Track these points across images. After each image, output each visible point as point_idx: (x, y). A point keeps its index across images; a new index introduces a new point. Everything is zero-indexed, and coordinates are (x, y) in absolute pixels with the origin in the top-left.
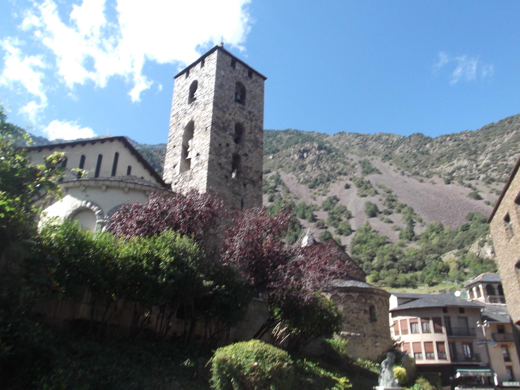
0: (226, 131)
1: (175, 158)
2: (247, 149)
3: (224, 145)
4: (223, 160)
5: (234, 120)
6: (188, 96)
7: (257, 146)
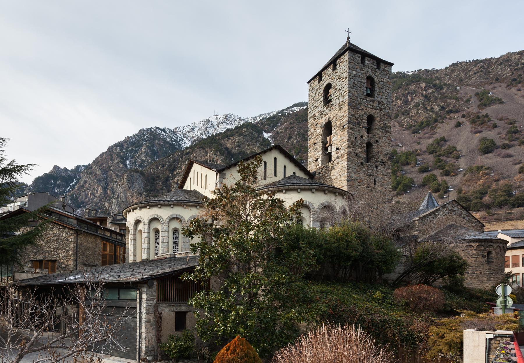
1: (316, 153)
3: (359, 137)
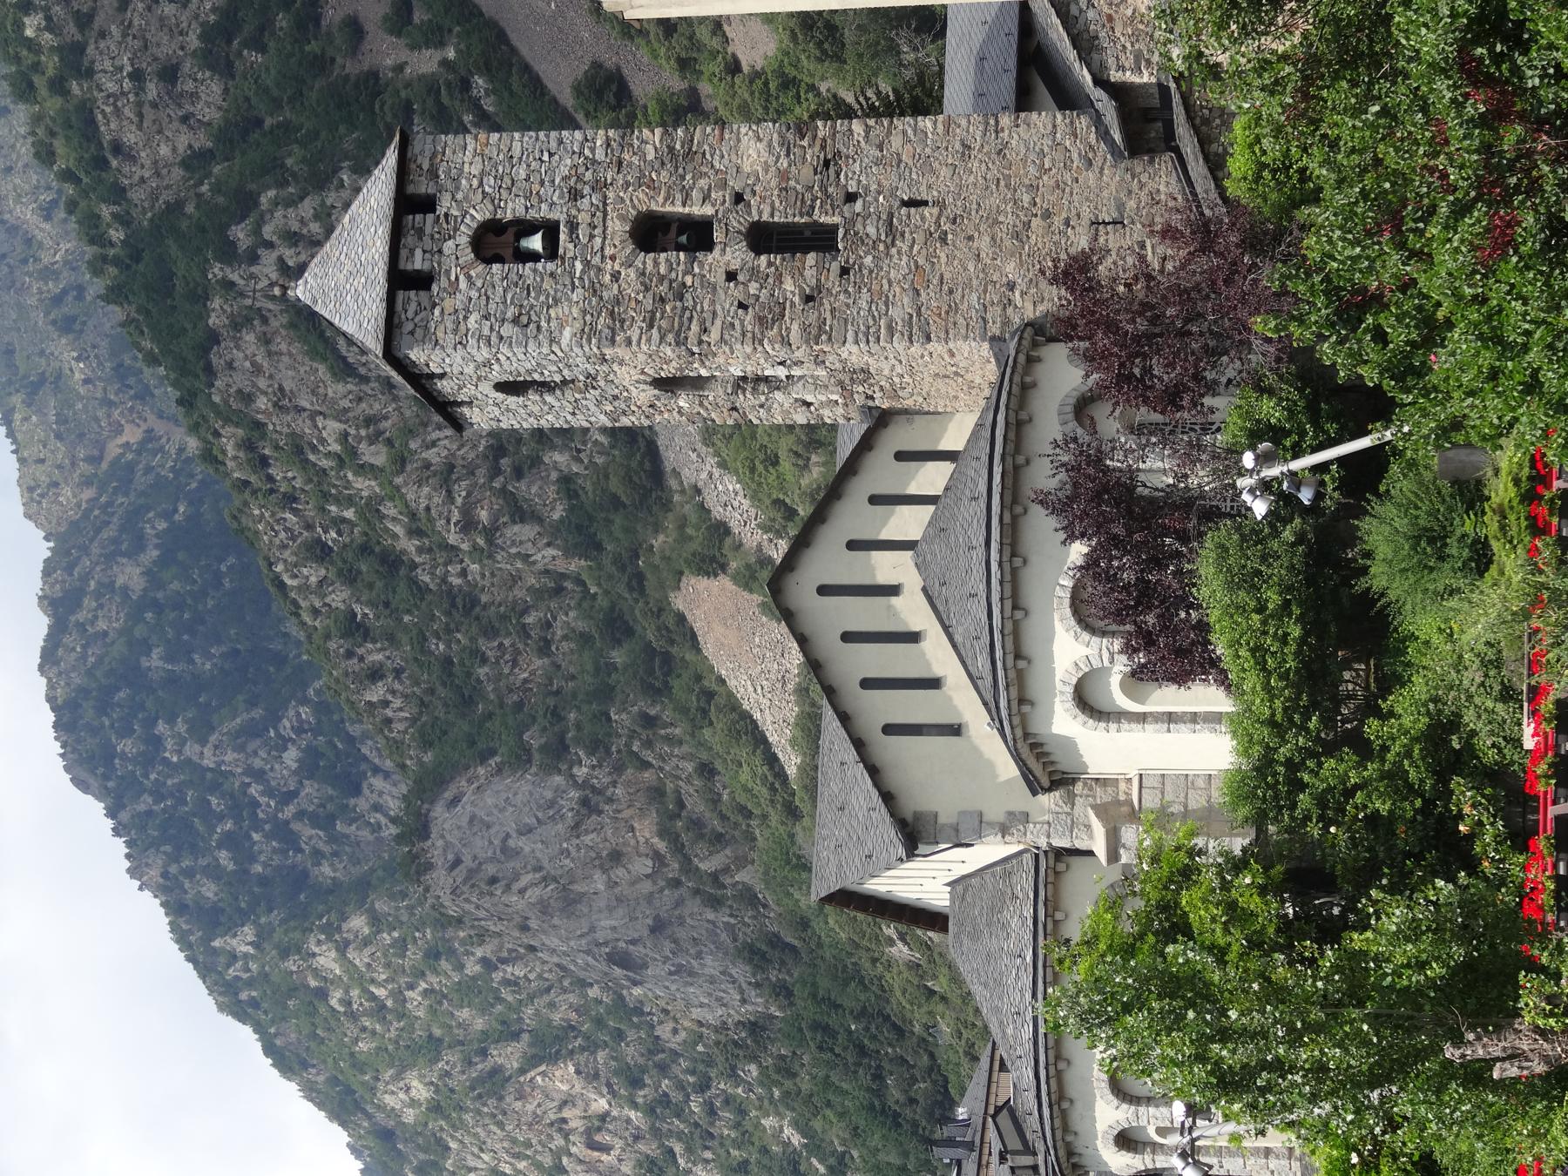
0: (684, 284)
3: (735, 291)
6: (549, 398)
7: (689, 154)
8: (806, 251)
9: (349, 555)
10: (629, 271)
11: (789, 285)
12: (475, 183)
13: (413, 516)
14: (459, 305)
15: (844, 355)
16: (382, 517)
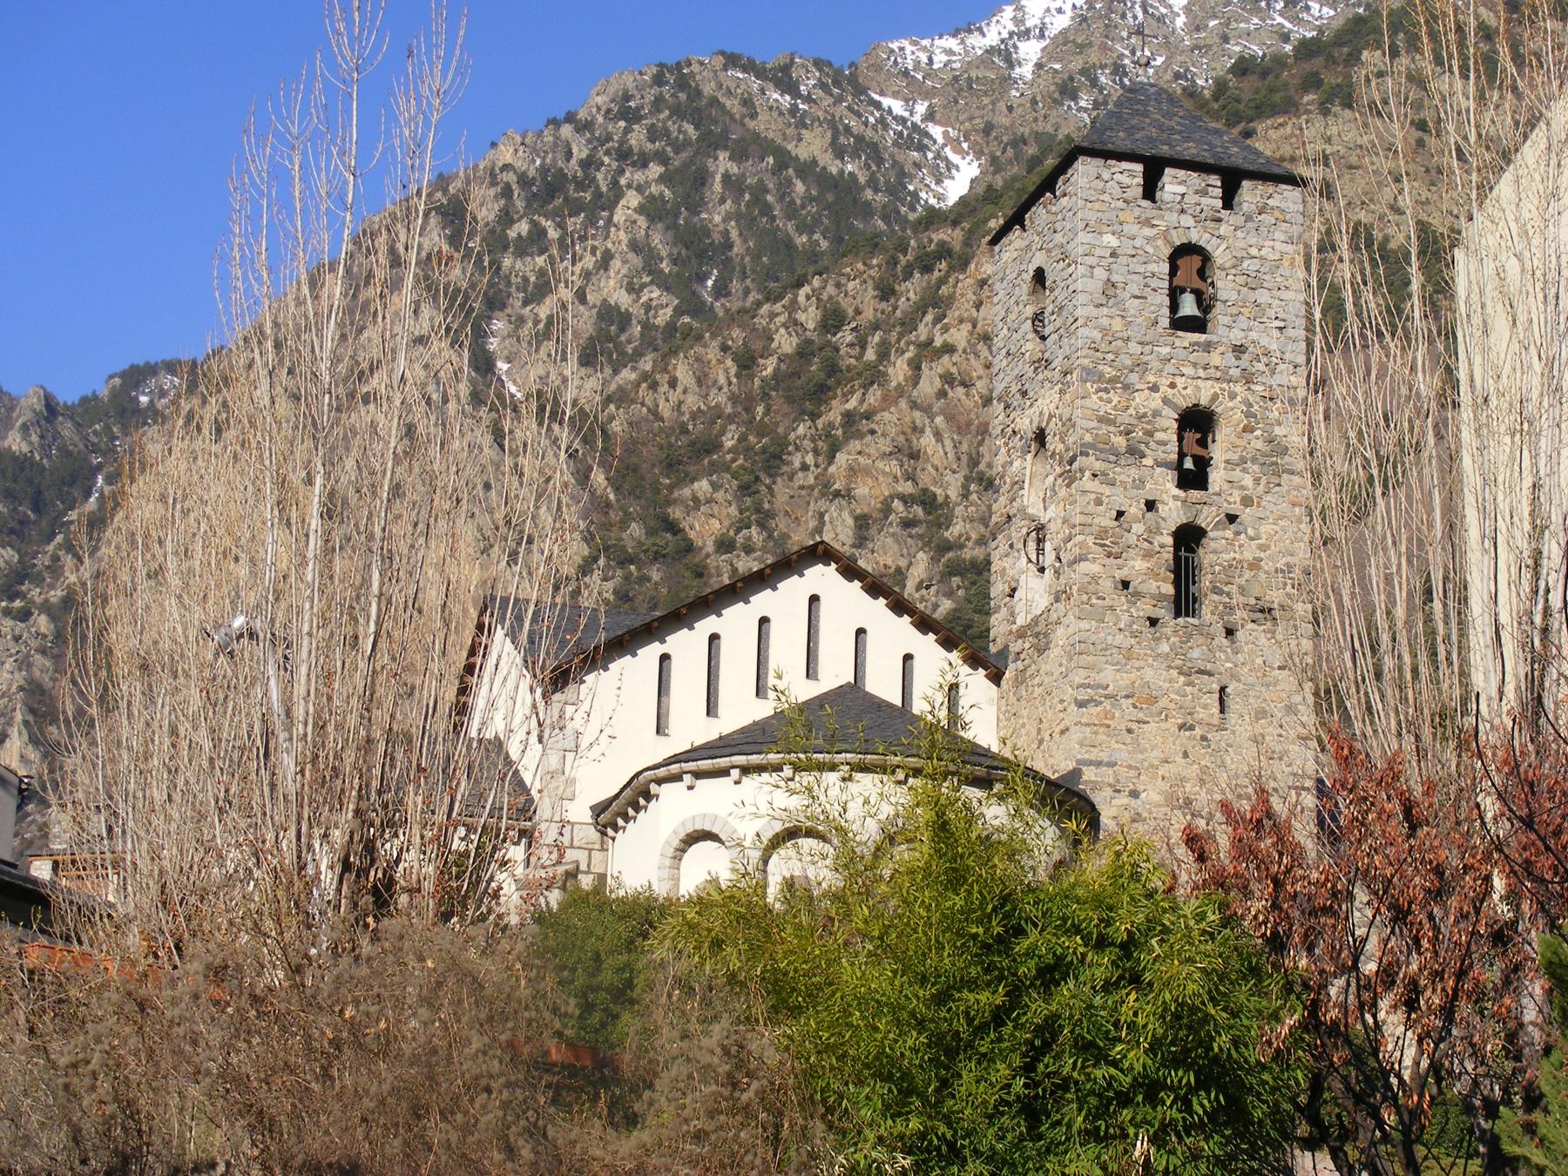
0: (1143, 456)
2: (1236, 496)
3: (1135, 509)
4: (1136, 566)
5: (1173, 406)
8: (1177, 583)
9: (827, 352)
10: (1157, 407)
11: (1140, 565)
12: (1254, 251)
13: (868, 416)
14: (1126, 228)
15: (1065, 621)
16: (866, 387)
